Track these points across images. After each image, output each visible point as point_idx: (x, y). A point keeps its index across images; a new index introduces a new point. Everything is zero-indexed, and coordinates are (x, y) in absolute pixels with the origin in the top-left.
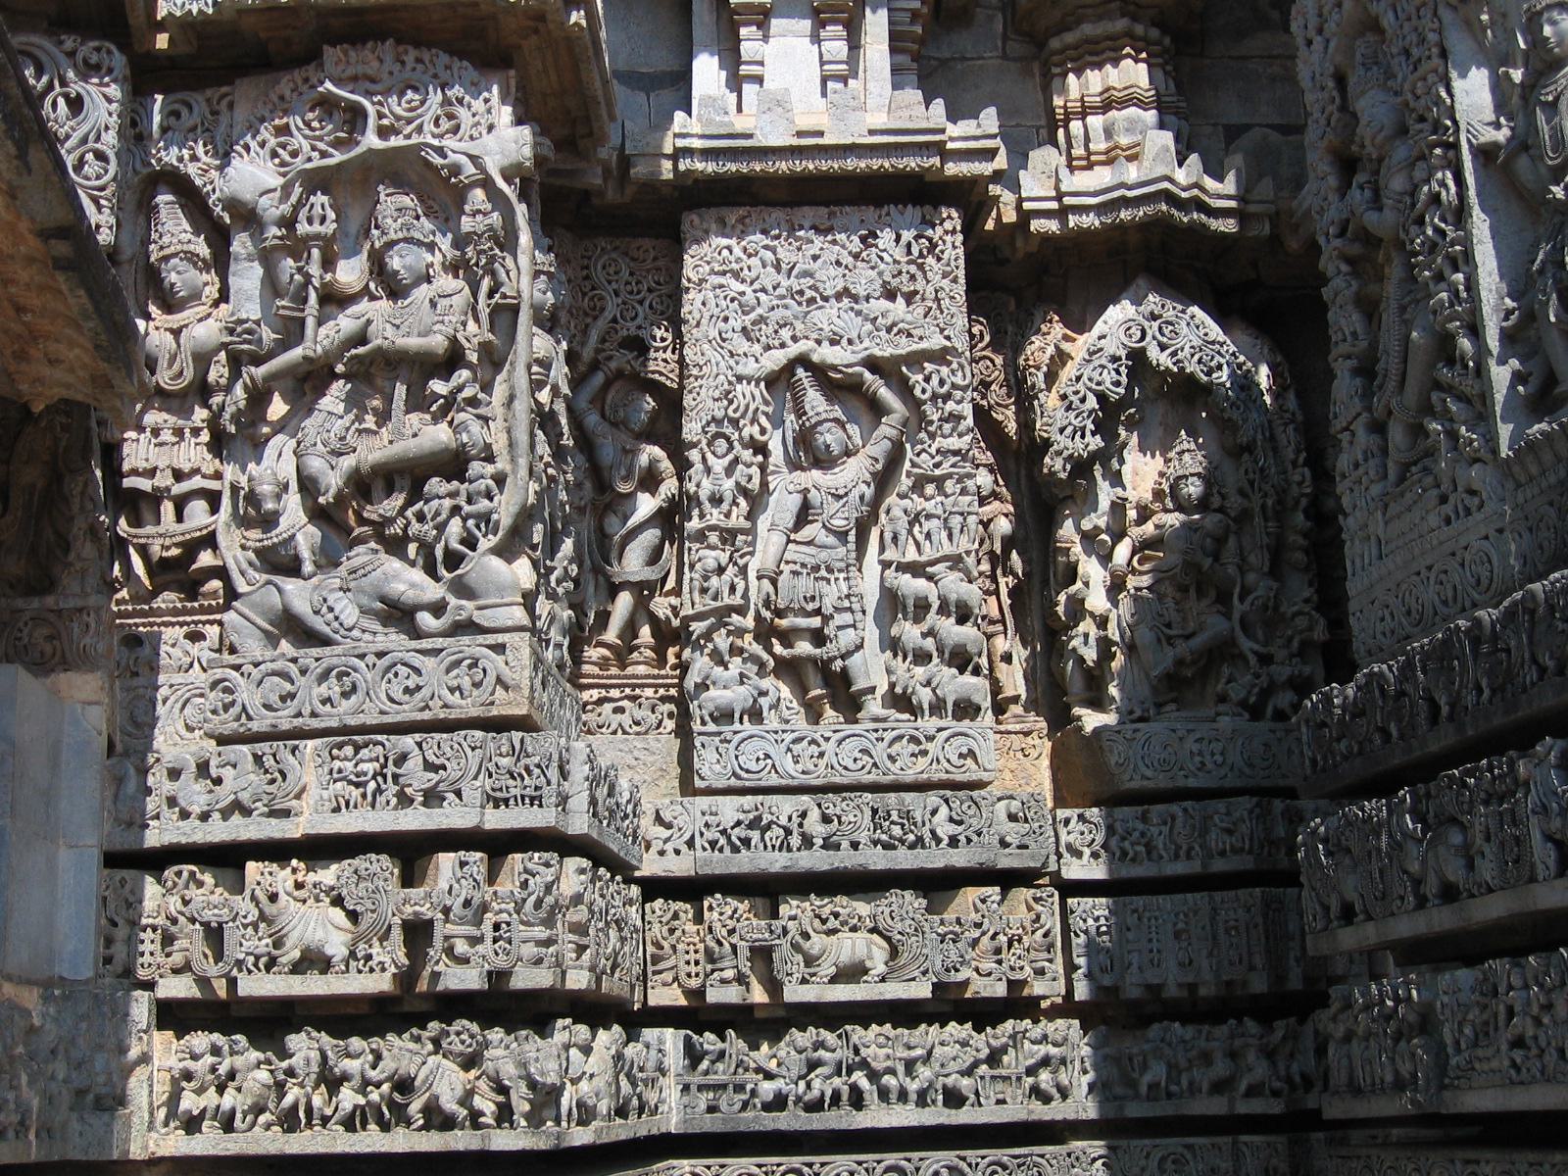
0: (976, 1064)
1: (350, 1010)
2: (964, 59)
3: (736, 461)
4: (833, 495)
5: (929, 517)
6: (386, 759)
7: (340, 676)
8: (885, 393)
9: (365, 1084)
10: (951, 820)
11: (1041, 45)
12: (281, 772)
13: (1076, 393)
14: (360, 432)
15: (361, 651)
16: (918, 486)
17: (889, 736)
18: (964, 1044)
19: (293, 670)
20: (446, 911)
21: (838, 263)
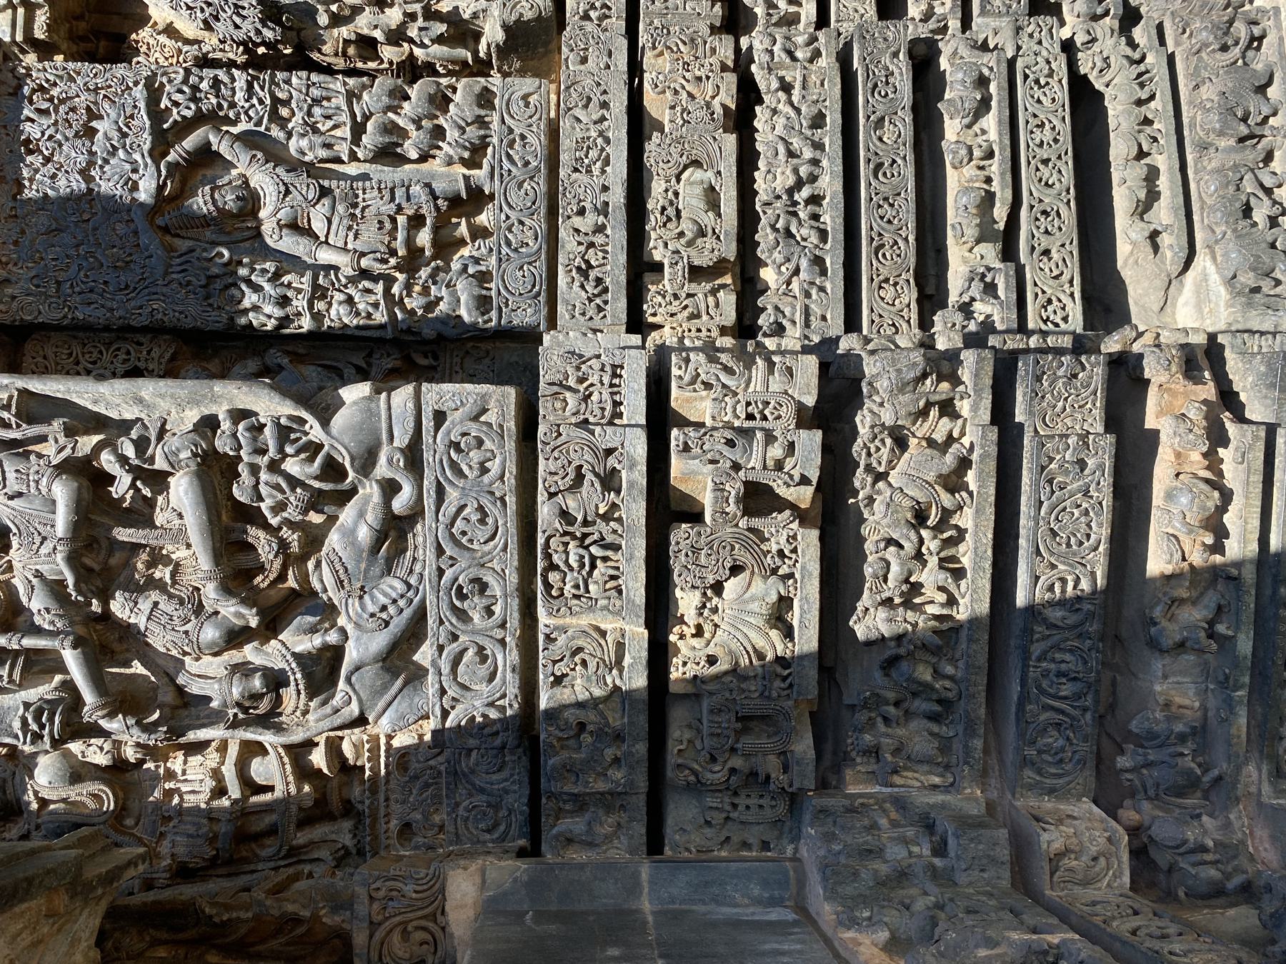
0: (792, 104)
3: (249, 282)
4: (285, 196)
5: (309, 114)
6: (566, 533)
7: (462, 596)
8: (190, 143)
9: (919, 556)
10: (586, 106)
12: (574, 654)
13: (202, 10)
14: (174, 582)
15: (435, 574)
16: (282, 122)
17: (506, 165)
18: (775, 111)
19: (454, 648)
20: (736, 467)
21: (54, 177)
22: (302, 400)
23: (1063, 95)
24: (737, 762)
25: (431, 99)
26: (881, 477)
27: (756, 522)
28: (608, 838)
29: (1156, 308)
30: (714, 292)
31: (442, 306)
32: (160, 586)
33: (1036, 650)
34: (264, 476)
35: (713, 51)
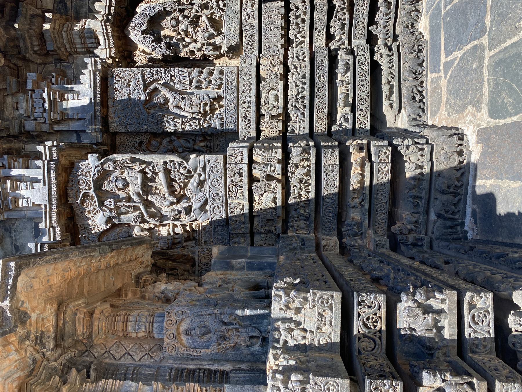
0: (297, 72)
1: (284, 194)
2: (73, 73)
3: (167, 121)
5: (179, 79)
7: (214, 196)
8: (152, 87)
9: (300, 189)
11: (70, 54)
16: (173, 81)
18: (293, 74)
19: (212, 206)
22: (183, 158)
23: (368, 67)
24: (266, 228)
25: (208, 73)
26: (292, 174)
27: (269, 182)
28: (243, 243)
29: (393, 122)
30: (277, 122)
31: (212, 126)
32: (157, 194)
33: (325, 207)
34: (176, 173)
35: (278, 58)
